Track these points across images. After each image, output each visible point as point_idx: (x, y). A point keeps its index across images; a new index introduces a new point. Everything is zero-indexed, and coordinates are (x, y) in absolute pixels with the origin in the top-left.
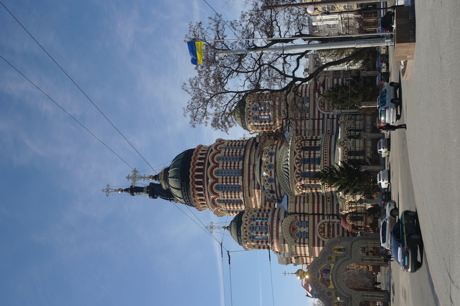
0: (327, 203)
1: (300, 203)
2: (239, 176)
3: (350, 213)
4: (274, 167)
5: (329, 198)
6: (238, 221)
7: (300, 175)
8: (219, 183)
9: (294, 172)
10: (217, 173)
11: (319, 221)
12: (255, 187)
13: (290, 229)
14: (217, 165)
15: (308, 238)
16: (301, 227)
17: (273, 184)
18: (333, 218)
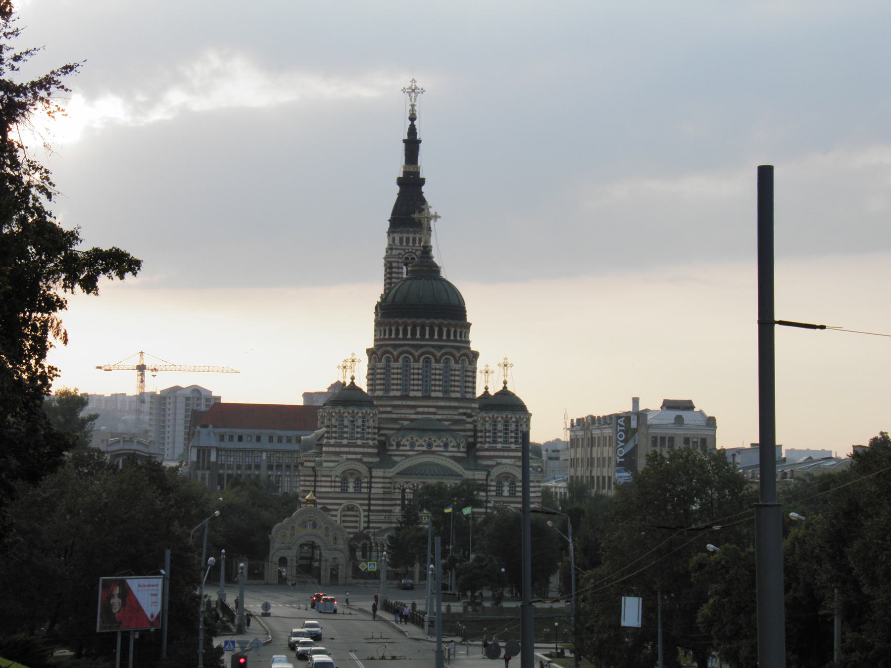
0: (384, 515)
1: (384, 483)
2: (423, 392)
3: (371, 543)
4: (430, 450)
5: (388, 518)
6: (361, 401)
7: (416, 488)
8: (413, 364)
9: (420, 482)
10: (427, 361)
11: (361, 505)
12: (406, 415)
13: (351, 469)
15: (341, 492)
16: (354, 482)
17: (408, 448)
18: (365, 522)
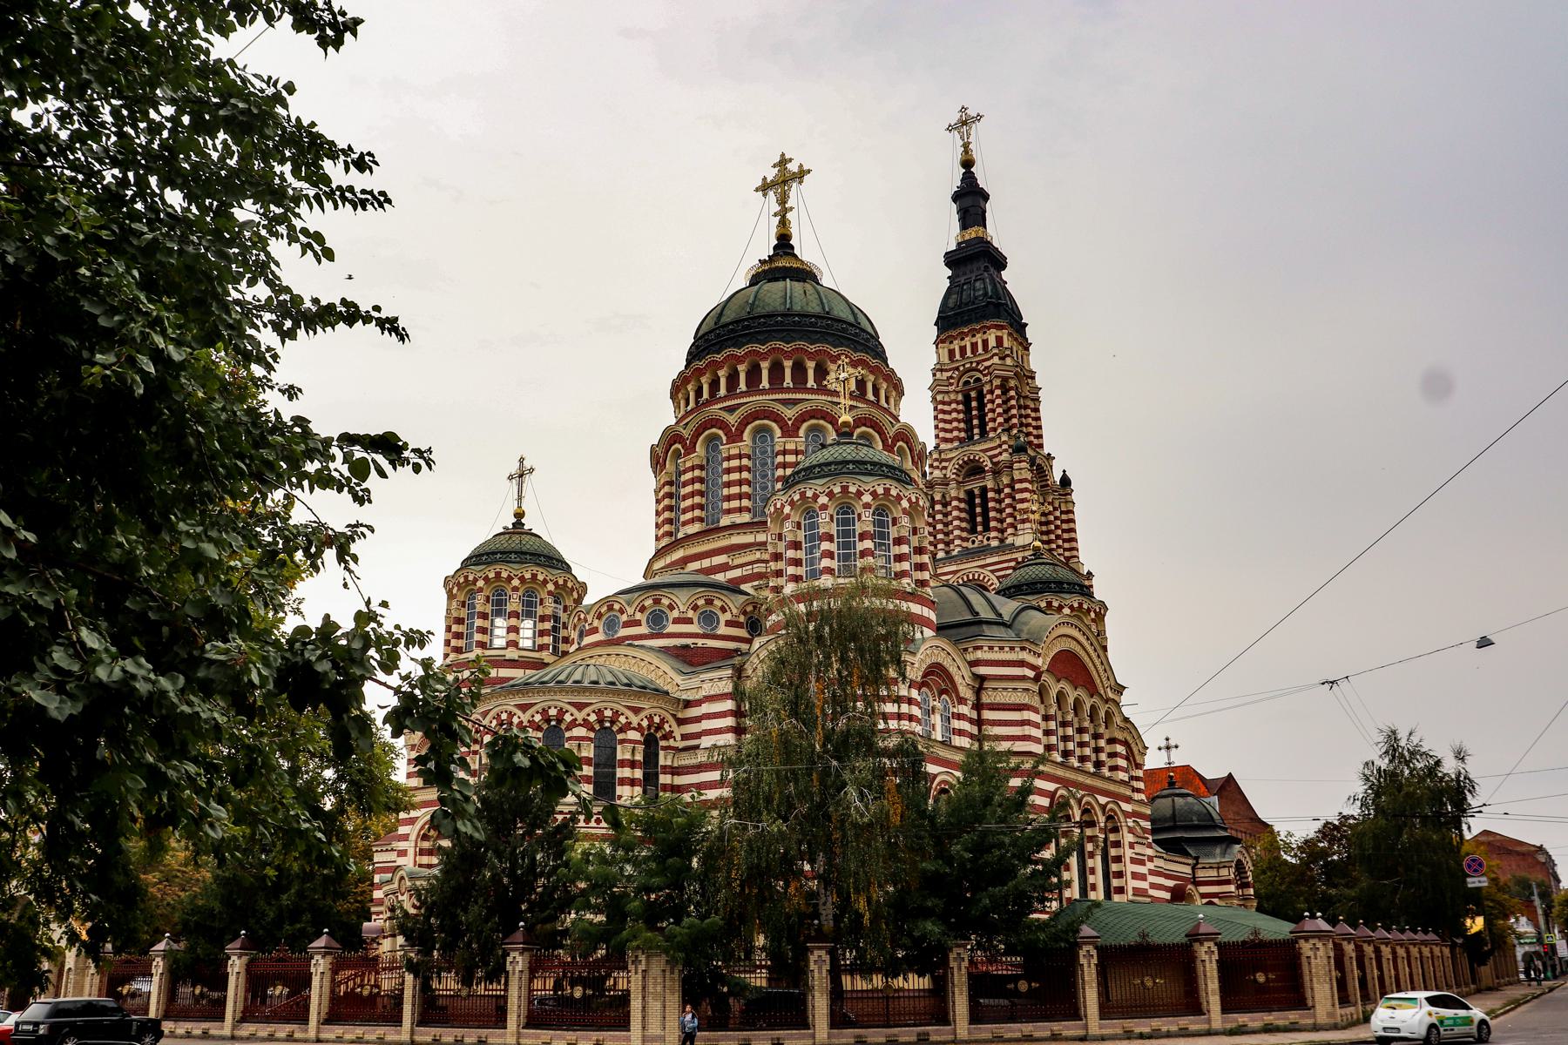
14: (790, 431)
